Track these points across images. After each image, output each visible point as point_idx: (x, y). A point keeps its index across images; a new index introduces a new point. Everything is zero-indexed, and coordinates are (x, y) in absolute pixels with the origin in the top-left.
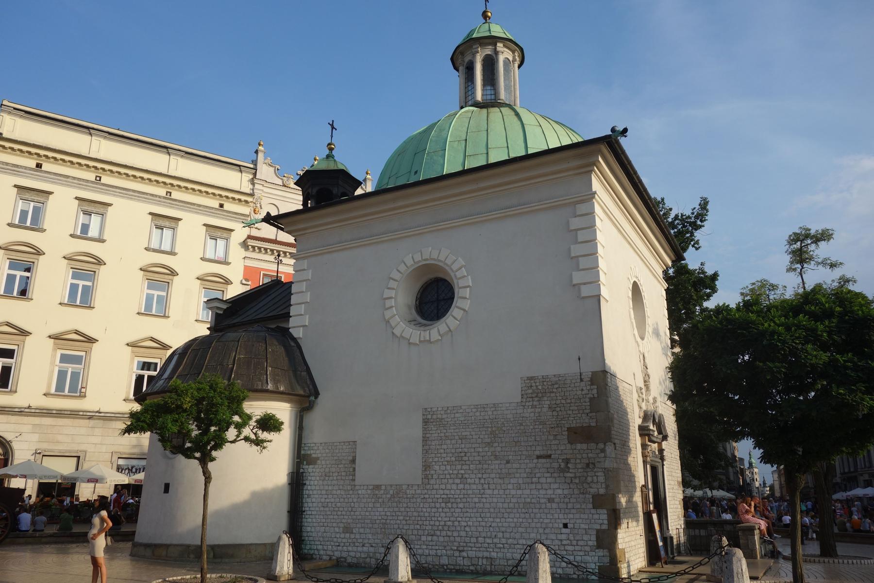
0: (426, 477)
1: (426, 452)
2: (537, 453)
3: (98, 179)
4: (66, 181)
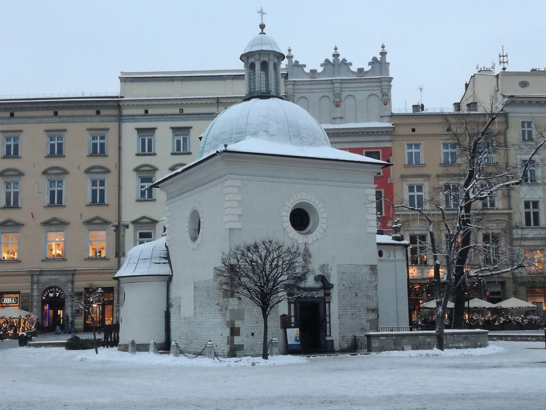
0: (195, 314)
1: (195, 301)
2: (217, 302)
3: (181, 111)
4: (163, 118)
